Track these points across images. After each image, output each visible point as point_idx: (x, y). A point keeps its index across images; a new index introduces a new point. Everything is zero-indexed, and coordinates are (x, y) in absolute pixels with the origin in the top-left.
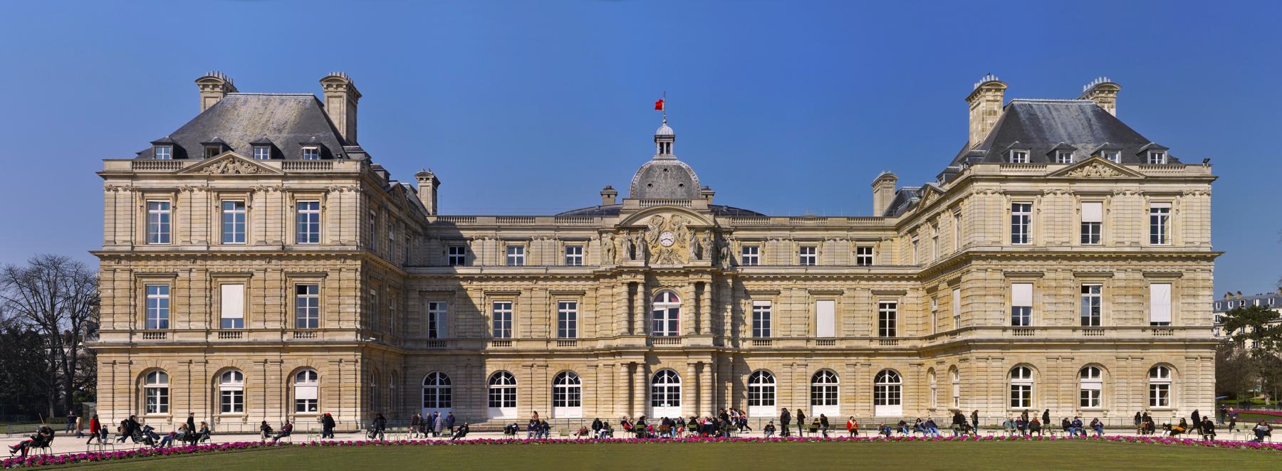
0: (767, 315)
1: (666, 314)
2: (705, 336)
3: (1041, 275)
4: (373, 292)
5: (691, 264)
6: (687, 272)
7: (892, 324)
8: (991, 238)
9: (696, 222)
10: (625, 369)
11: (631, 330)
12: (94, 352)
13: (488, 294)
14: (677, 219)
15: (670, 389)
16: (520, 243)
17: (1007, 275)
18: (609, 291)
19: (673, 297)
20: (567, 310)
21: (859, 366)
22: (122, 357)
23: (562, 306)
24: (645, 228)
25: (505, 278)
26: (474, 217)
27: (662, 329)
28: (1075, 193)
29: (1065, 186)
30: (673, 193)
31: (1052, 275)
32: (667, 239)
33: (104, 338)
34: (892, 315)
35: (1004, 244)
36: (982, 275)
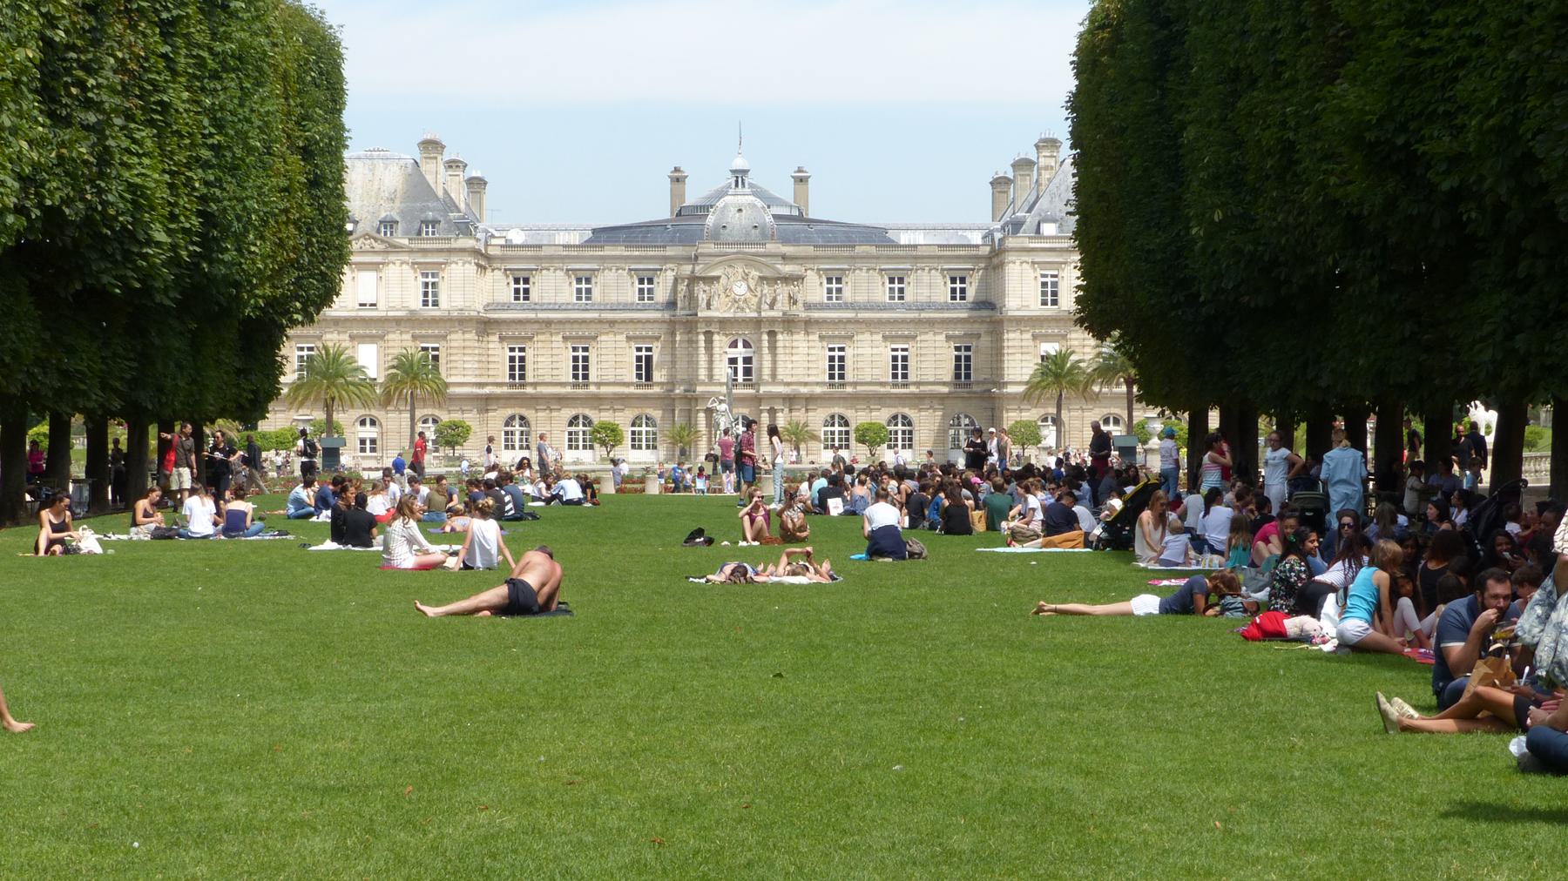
1: (740, 361)
3: (1064, 337)
6: (758, 323)
7: (968, 367)
9: (767, 273)
10: (702, 415)
17: (1035, 337)
18: (686, 337)
19: (746, 345)
23: (639, 349)
24: (717, 278)
25: (584, 321)
26: (540, 246)
30: (748, 234)
32: (740, 289)
34: (968, 358)
36: (1011, 335)
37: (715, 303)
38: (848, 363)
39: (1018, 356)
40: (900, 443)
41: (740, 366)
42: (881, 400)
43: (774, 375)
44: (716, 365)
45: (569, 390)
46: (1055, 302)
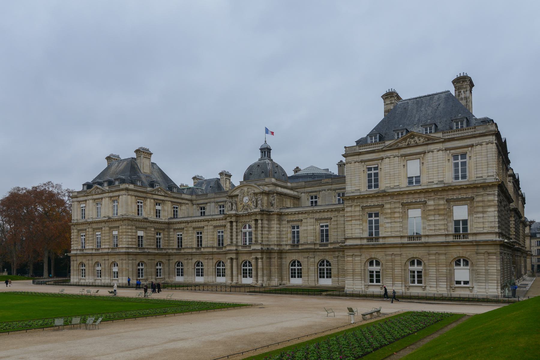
0: (298, 232)
2: (259, 245)
3: (382, 206)
4: (141, 233)
5: (252, 211)
8: (354, 188)
9: (257, 191)
10: (229, 261)
11: (232, 242)
12: (69, 257)
13: (194, 228)
14: (249, 190)
15: (249, 269)
16: (222, 203)
17: (363, 208)
19: (250, 227)
20: (221, 234)
21: (339, 258)
22: (74, 258)
23: (219, 232)
24: (237, 195)
27: (246, 242)
28: (362, 161)
29: (396, 153)
31: (387, 206)
32: (246, 199)
33: (73, 252)
35: (362, 190)
36: (349, 209)
37: (233, 207)
38: (301, 234)
39: (354, 222)
40: (325, 275)
41: (248, 237)
42: (315, 251)
43: (256, 241)
44: (234, 237)
45: (194, 250)
46: (376, 186)
